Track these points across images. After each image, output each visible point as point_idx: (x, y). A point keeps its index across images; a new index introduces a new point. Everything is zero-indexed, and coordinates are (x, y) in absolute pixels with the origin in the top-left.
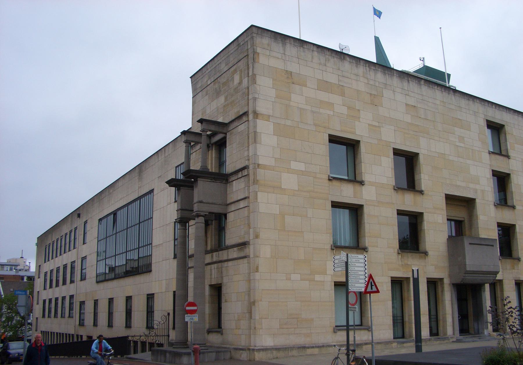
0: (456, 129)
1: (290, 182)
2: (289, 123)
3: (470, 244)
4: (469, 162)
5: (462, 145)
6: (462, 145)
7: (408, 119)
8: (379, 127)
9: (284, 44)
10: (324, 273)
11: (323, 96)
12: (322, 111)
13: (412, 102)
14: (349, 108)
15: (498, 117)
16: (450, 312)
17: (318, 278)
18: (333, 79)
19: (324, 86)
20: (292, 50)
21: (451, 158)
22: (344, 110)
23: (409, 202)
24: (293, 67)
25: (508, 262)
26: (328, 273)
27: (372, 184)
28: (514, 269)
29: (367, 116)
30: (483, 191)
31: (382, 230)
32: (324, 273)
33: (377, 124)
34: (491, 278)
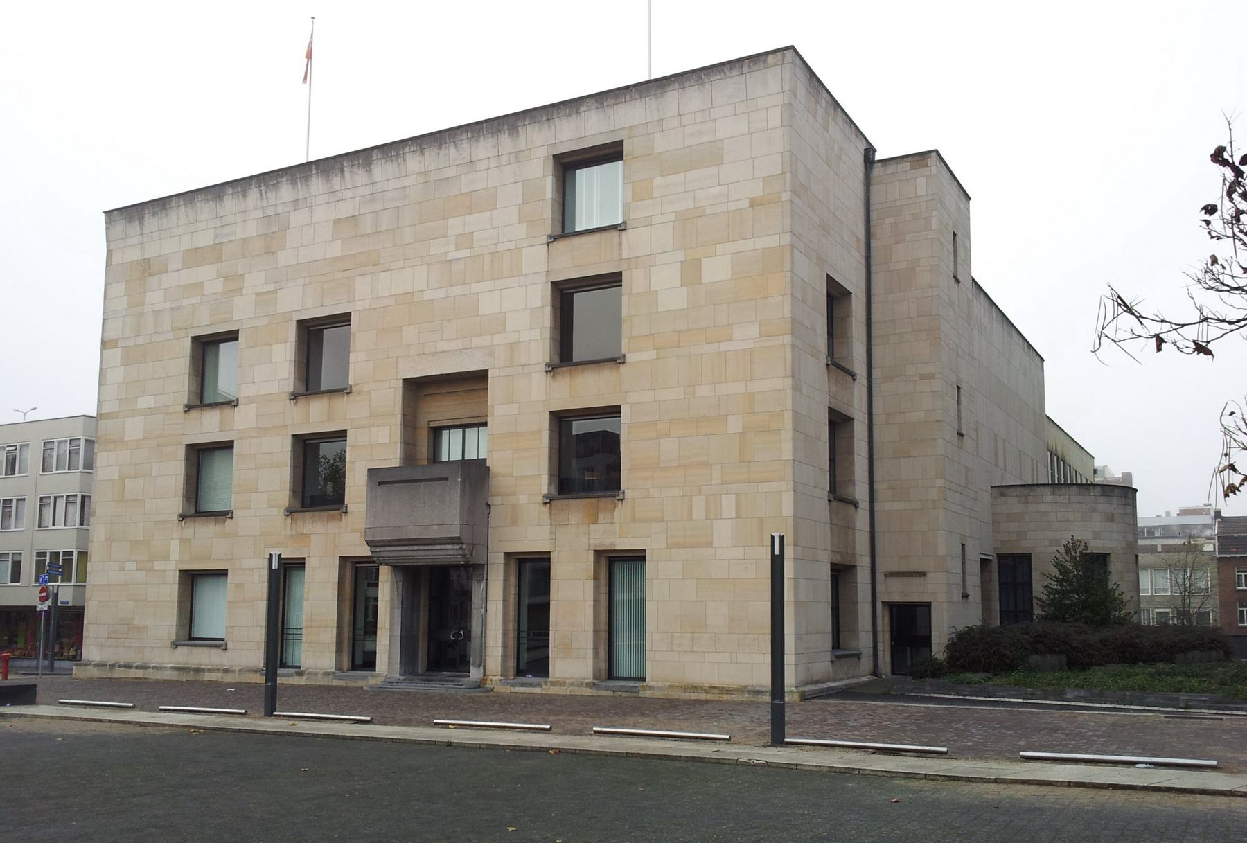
0: (451, 221)
1: (134, 428)
2: (140, 340)
3: (380, 484)
4: (476, 288)
5: (465, 253)
6: (465, 253)
7: (336, 250)
8: (275, 291)
9: (141, 219)
10: (166, 558)
11: (189, 277)
12: (186, 302)
13: (345, 210)
14: (226, 278)
15: (591, 130)
16: (387, 625)
17: (158, 566)
18: (205, 239)
19: (195, 257)
20: (151, 223)
21: (427, 296)
22: (219, 286)
23: (316, 416)
24: (153, 250)
25: (576, 509)
26: (172, 557)
27: (250, 400)
28: (595, 522)
29: (255, 281)
30: (513, 347)
31: (259, 480)
32: (166, 558)
33: (271, 287)
34: (451, 552)
